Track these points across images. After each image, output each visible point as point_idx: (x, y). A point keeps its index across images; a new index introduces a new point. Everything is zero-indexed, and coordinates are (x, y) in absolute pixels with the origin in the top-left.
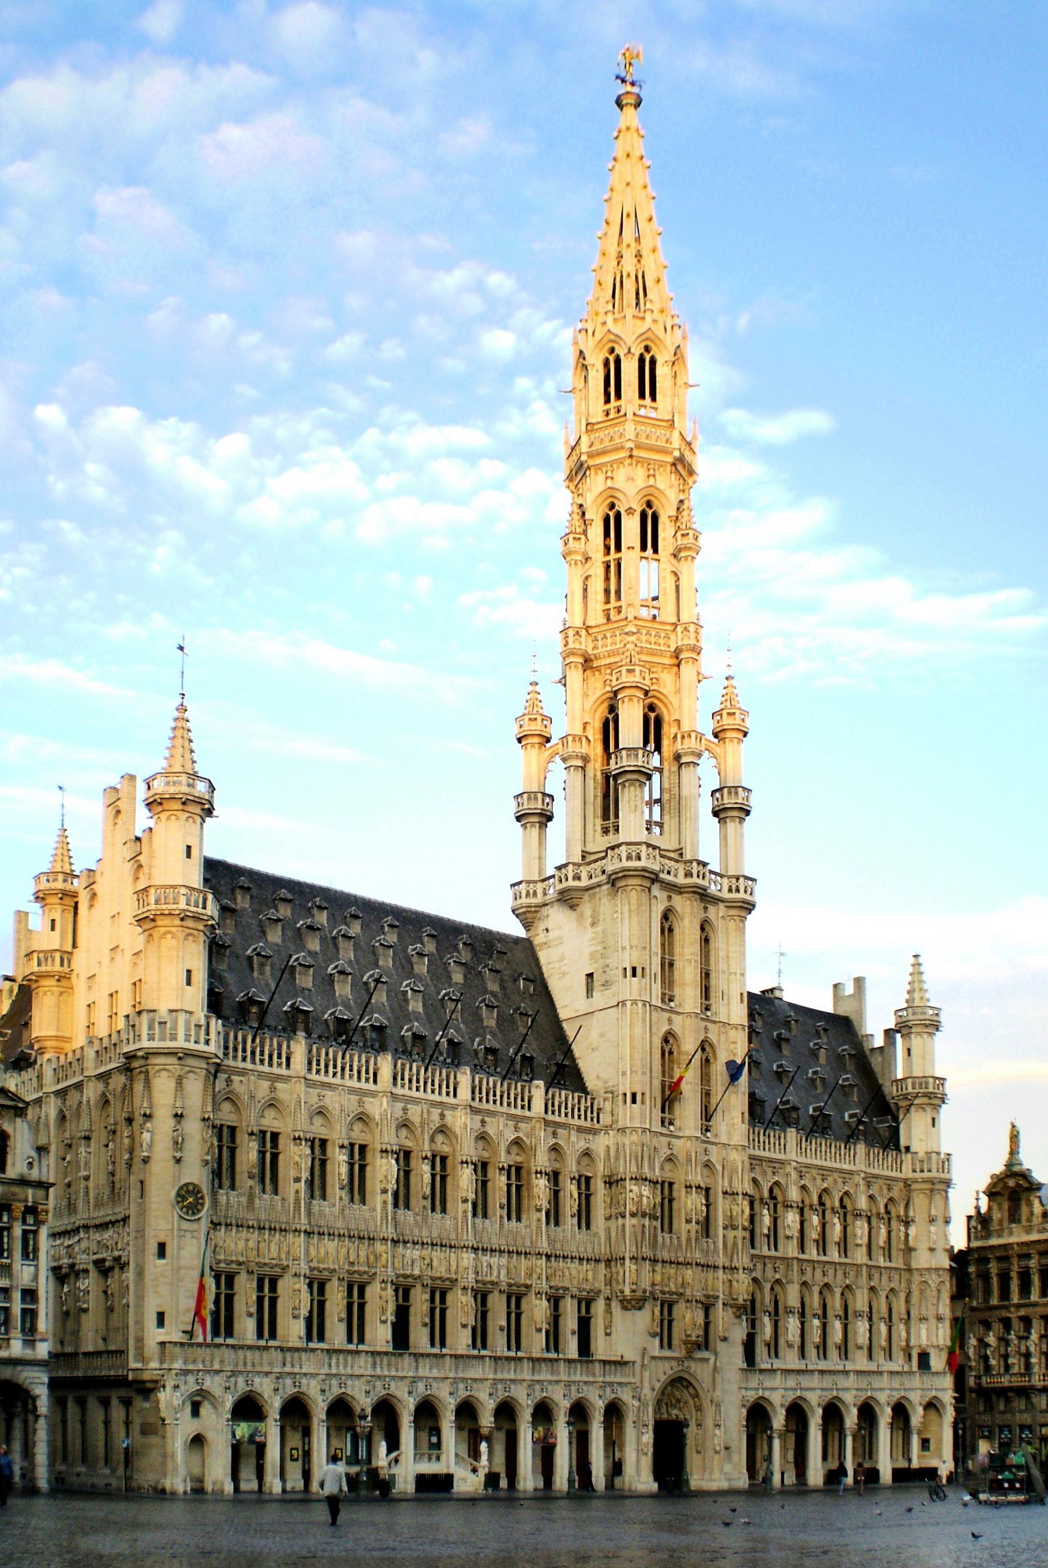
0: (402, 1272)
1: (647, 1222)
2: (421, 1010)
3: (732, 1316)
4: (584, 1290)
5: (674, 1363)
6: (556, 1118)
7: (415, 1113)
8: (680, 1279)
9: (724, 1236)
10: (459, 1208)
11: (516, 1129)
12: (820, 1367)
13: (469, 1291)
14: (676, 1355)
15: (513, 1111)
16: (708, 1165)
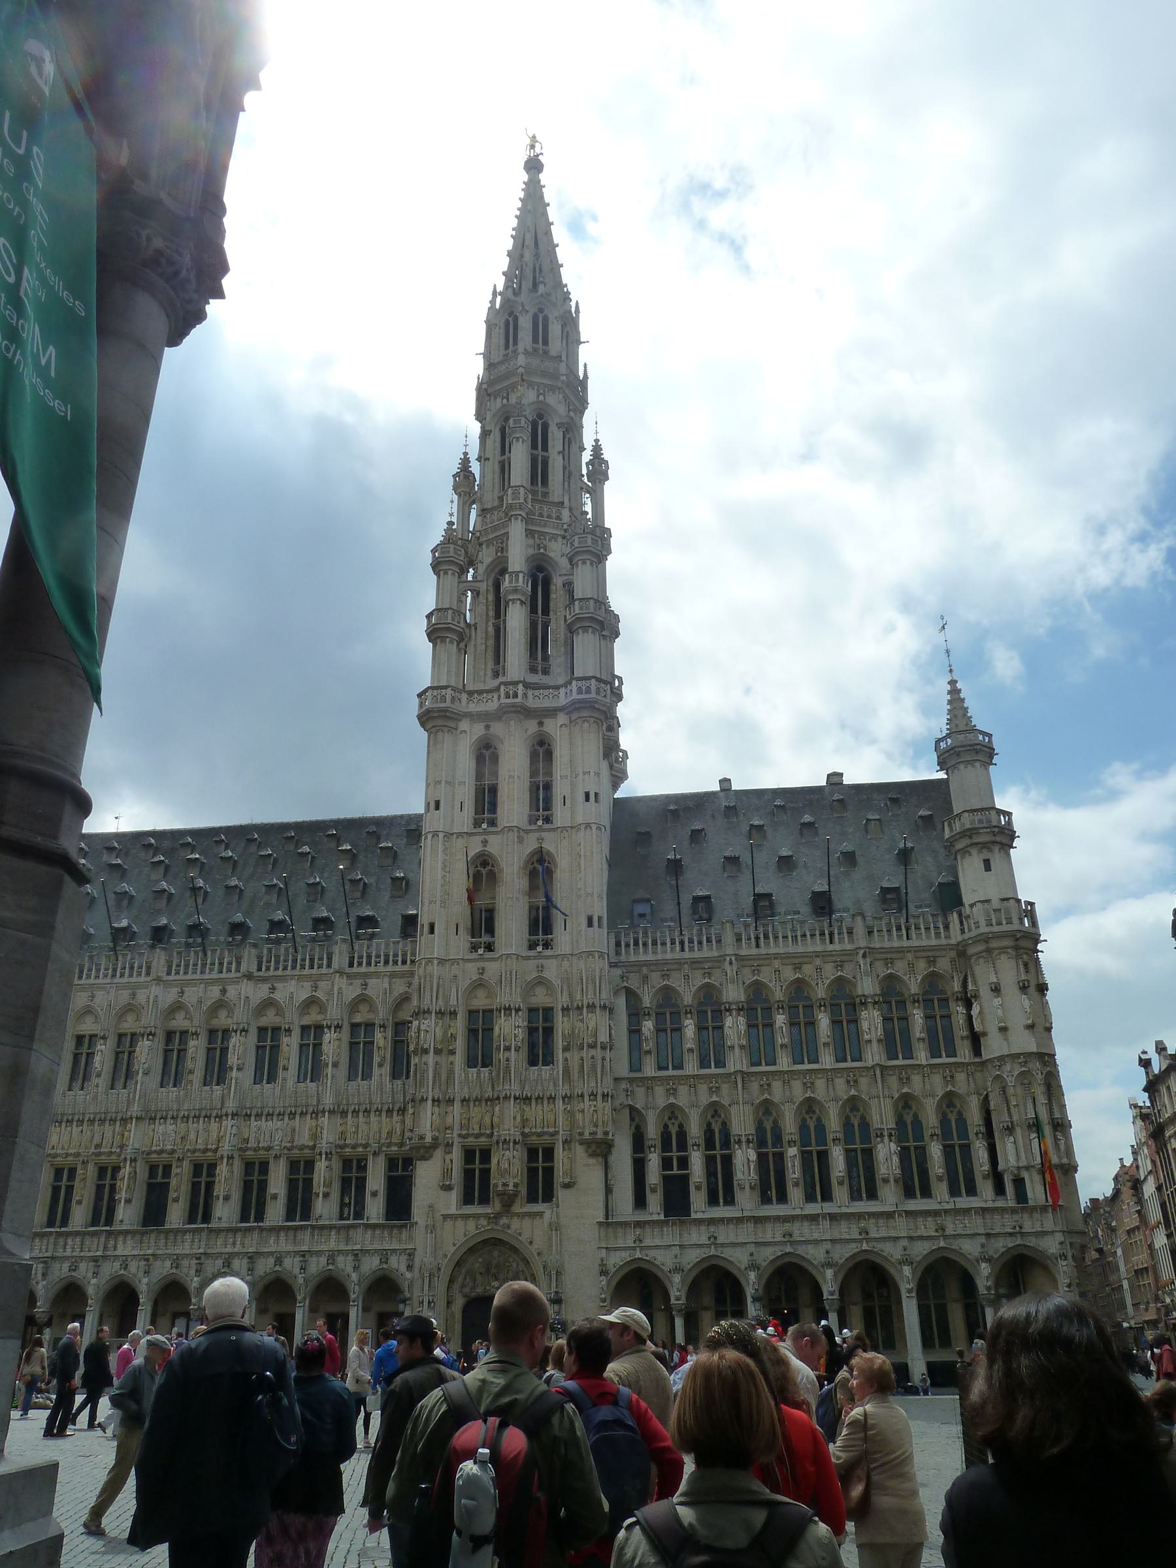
0: (154, 1148)
1: (430, 1058)
2: (274, 901)
3: (584, 1155)
4: (389, 1145)
5: (483, 1222)
6: (363, 969)
7: (192, 996)
8: (487, 1120)
9: (566, 1060)
10: (241, 1076)
11: (315, 988)
12: (806, 1212)
13: (225, 1160)
14: (489, 1210)
15: (307, 971)
16: (541, 982)
